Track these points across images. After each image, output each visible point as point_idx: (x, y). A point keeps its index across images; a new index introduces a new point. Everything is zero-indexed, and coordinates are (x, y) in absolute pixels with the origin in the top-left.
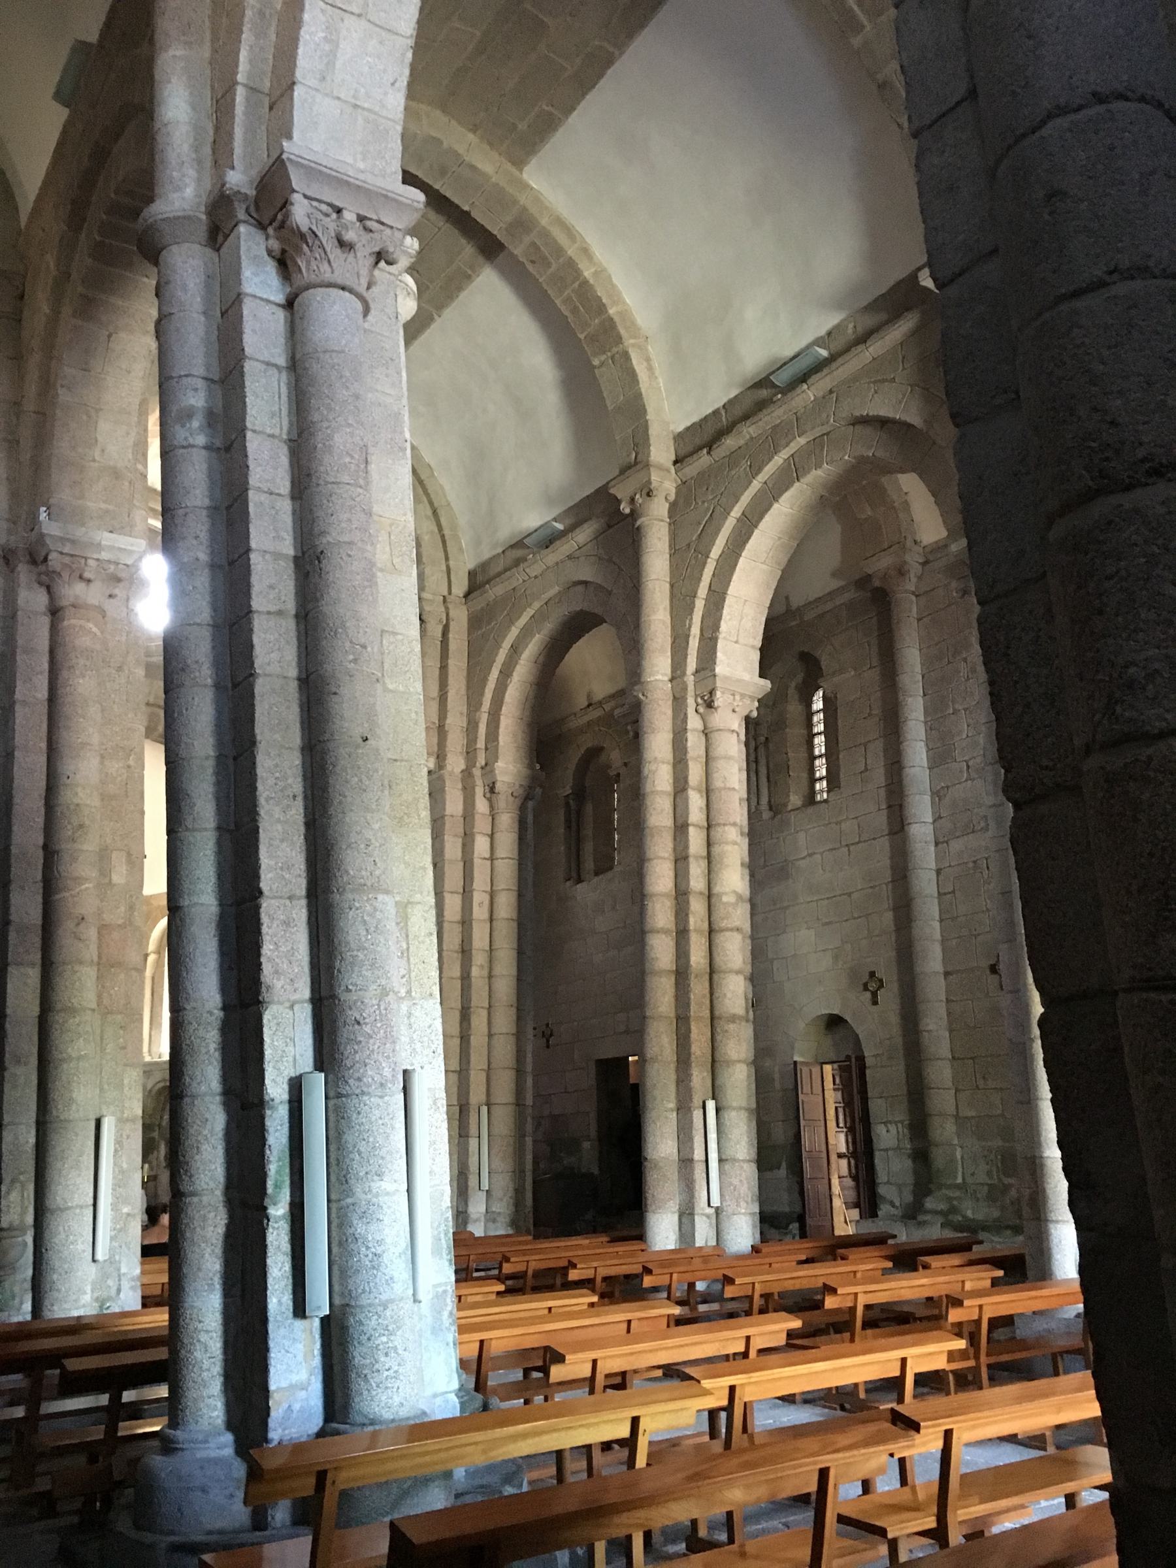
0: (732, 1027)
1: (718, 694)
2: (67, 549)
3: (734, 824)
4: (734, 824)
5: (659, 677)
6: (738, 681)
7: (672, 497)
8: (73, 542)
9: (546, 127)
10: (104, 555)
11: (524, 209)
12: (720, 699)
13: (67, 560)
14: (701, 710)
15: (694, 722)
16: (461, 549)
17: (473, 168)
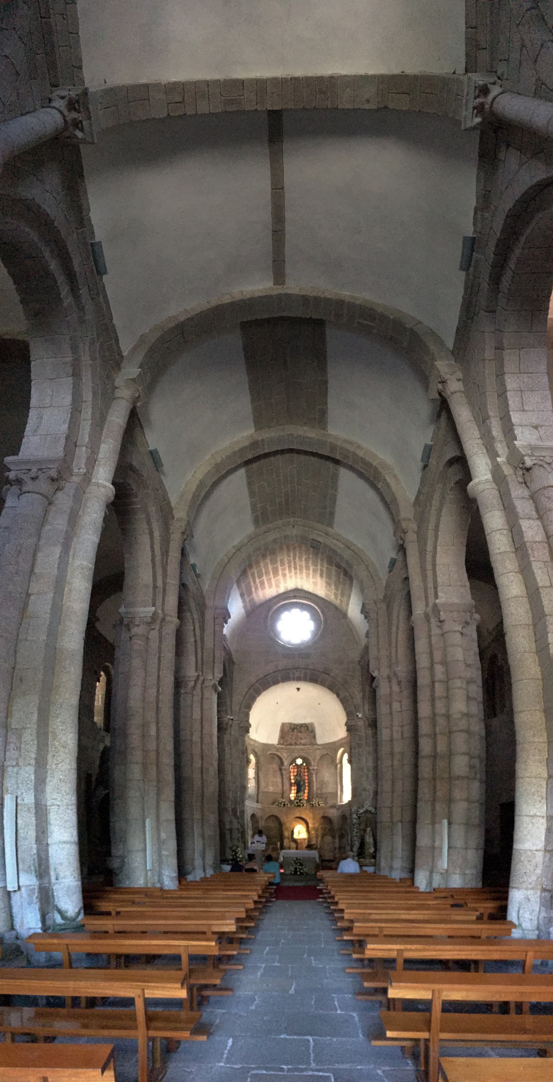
0: (457, 782)
1: (442, 613)
2: (129, 616)
3: (460, 678)
4: (460, 678)
5: (419, 612)
6: (451, 605)
7: (416, 529)
8: (130, 613)
9: (323, 413)
10: (142, 615)
11: (331, 443)
12: (443, 616)
13: (130, 619)
14: (439, 624)
15: (436, 631)
16: (380, 579)
17: (309, 438)
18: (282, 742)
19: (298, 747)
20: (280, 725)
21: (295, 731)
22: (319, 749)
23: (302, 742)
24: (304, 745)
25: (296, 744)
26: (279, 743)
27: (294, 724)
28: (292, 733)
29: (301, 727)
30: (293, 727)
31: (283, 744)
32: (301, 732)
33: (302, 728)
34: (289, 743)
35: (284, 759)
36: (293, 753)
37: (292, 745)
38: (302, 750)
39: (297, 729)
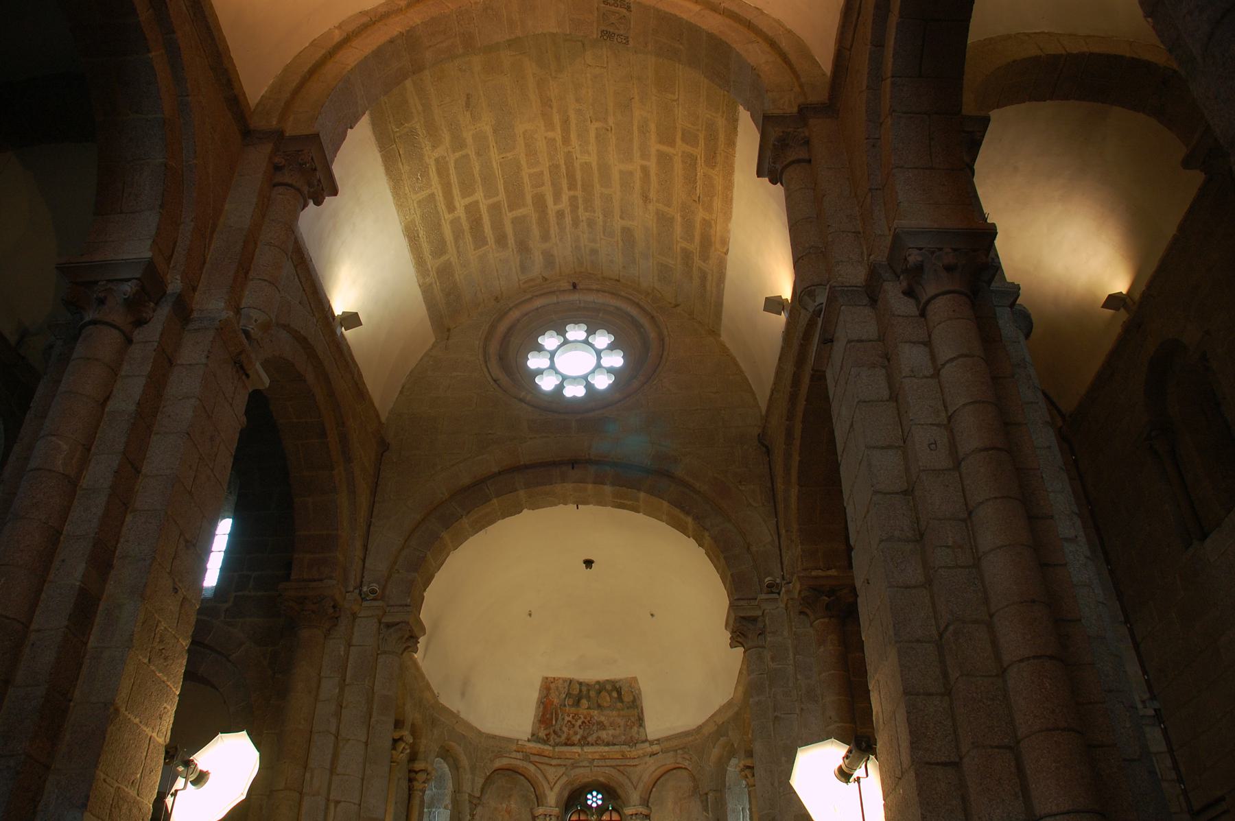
18: (542, 734)
19: (587, 749)
20: (538, 685)
21: (584, 702)
22: (653, 754)
23: (603, 734)
24: (608, 744)
25: (584, 742)
26: (534, 737)
27: (581, 684)
28: (573, 710)
29: (599, 692)
30: (576, 692)
31: (545, 742)
32: (599, 706)
33: (604, 693)
34: (564, 737)
35: (546, 785)
36: (574, 766)
37: (573, 745)
38: (604, 758)
39: (589, 698)
